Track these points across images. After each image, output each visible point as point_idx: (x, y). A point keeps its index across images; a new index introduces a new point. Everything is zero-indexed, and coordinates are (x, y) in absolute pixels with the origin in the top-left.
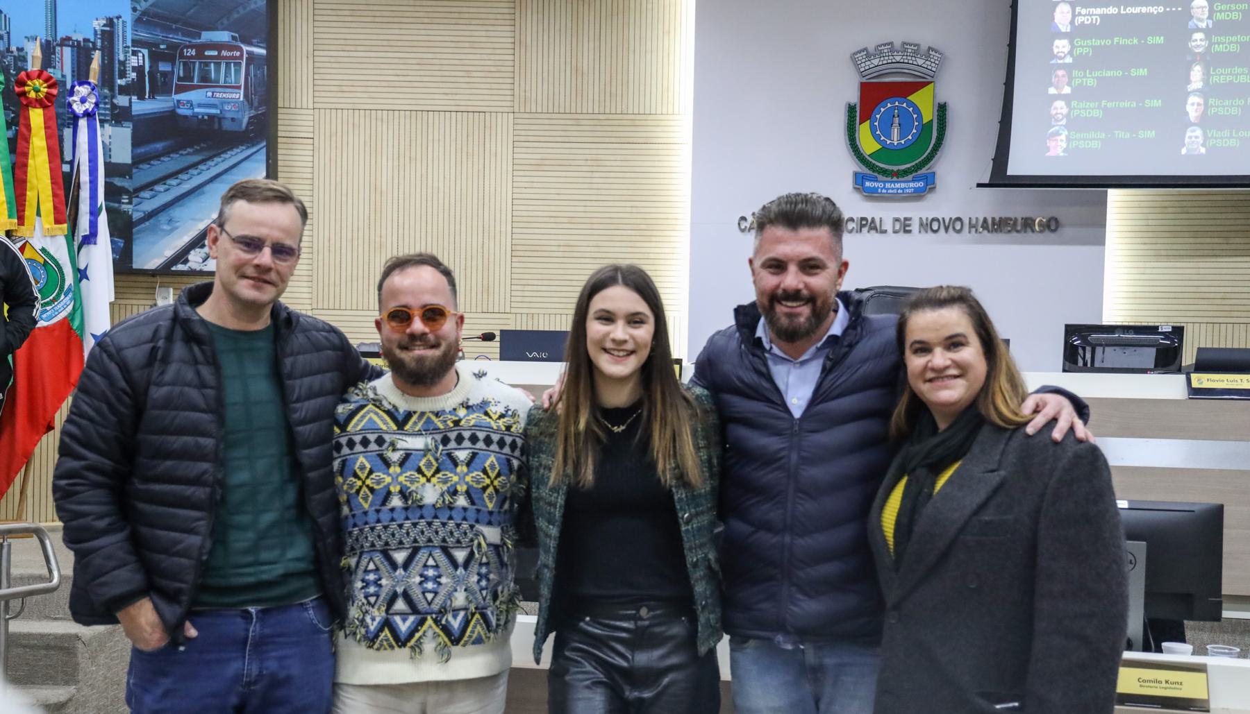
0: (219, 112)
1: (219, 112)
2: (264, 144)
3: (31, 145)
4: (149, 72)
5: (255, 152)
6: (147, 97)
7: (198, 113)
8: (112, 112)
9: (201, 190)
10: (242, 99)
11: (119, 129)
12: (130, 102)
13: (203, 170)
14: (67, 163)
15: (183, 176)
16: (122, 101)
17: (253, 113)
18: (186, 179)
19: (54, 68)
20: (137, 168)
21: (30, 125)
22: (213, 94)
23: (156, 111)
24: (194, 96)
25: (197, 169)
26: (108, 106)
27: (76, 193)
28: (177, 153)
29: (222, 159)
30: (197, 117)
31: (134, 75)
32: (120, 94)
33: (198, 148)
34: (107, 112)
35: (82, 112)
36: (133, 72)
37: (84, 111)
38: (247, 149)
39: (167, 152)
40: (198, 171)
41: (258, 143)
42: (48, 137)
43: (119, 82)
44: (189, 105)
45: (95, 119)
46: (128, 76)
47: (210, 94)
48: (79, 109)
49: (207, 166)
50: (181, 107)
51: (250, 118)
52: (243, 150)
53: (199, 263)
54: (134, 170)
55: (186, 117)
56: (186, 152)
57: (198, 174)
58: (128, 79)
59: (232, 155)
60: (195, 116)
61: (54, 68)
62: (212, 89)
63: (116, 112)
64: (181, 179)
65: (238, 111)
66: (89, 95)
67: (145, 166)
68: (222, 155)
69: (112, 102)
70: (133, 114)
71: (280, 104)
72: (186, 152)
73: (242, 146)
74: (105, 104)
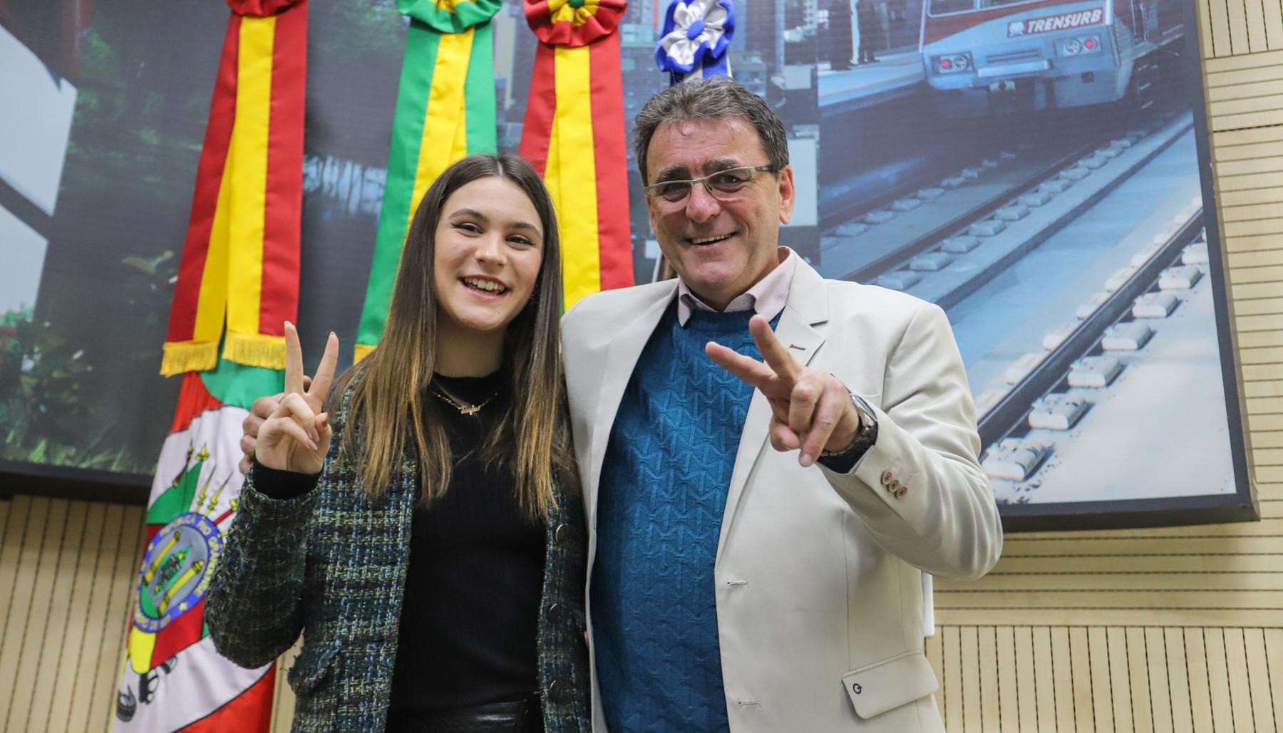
0: (1045, 65)
1: (1045, 65)
2: (1189, 119)
3: (553, 141)
4: (858, 7)
5: (1160, 150)
6: (855, 60)
7: (991, 79)
9: (1009, 271)
10: (1108, 20)
12: (814, 78)
13: (1012, 220)
15: (955, 243)
17: (1145, 48)
18: (964, 248)
19: (638, 21)
20: (832, 235)
22: (1027, 25)
23: (878, 90)
24: (973, 40)
25: (992, 218)
28: (938, 186)
29: (1066, 182)
30: (987, 88)
31: (823, 16)
32: (789, 62)
33: (994, 164)
35: (691, 61)
36: (820, 8)
37: (697, 55)
38: (1132, 145)
39: (907, 188)
40: (997, 223)
41: (1167, 122)
42: (597, 115)
43: (788, 35)
44: (963, 63)
45: (725, 68)
46: (808, 19)
47: (1017, 27)
48: (683, 55)
49: (1020, 209)
50: (942, 71)
51: (1137, 63)
52: (1125, 148)
53: (1015, 481)
54: (825, 242)
55: (955, 93)
56: (960, 180)
57: (998, 232)
58: (808, 27)
59: (1091, 169)
60: (982, 87)
61: (638, 21)
62: (1024, 15)
64: (950, 252)
65: (1101, 54)
66: (709, 13)
67: (853, 229)
68: (1062, 173)
70: (821, 104)
71: (1208, 52)
72: (960, 180)
73: (1120, 138)
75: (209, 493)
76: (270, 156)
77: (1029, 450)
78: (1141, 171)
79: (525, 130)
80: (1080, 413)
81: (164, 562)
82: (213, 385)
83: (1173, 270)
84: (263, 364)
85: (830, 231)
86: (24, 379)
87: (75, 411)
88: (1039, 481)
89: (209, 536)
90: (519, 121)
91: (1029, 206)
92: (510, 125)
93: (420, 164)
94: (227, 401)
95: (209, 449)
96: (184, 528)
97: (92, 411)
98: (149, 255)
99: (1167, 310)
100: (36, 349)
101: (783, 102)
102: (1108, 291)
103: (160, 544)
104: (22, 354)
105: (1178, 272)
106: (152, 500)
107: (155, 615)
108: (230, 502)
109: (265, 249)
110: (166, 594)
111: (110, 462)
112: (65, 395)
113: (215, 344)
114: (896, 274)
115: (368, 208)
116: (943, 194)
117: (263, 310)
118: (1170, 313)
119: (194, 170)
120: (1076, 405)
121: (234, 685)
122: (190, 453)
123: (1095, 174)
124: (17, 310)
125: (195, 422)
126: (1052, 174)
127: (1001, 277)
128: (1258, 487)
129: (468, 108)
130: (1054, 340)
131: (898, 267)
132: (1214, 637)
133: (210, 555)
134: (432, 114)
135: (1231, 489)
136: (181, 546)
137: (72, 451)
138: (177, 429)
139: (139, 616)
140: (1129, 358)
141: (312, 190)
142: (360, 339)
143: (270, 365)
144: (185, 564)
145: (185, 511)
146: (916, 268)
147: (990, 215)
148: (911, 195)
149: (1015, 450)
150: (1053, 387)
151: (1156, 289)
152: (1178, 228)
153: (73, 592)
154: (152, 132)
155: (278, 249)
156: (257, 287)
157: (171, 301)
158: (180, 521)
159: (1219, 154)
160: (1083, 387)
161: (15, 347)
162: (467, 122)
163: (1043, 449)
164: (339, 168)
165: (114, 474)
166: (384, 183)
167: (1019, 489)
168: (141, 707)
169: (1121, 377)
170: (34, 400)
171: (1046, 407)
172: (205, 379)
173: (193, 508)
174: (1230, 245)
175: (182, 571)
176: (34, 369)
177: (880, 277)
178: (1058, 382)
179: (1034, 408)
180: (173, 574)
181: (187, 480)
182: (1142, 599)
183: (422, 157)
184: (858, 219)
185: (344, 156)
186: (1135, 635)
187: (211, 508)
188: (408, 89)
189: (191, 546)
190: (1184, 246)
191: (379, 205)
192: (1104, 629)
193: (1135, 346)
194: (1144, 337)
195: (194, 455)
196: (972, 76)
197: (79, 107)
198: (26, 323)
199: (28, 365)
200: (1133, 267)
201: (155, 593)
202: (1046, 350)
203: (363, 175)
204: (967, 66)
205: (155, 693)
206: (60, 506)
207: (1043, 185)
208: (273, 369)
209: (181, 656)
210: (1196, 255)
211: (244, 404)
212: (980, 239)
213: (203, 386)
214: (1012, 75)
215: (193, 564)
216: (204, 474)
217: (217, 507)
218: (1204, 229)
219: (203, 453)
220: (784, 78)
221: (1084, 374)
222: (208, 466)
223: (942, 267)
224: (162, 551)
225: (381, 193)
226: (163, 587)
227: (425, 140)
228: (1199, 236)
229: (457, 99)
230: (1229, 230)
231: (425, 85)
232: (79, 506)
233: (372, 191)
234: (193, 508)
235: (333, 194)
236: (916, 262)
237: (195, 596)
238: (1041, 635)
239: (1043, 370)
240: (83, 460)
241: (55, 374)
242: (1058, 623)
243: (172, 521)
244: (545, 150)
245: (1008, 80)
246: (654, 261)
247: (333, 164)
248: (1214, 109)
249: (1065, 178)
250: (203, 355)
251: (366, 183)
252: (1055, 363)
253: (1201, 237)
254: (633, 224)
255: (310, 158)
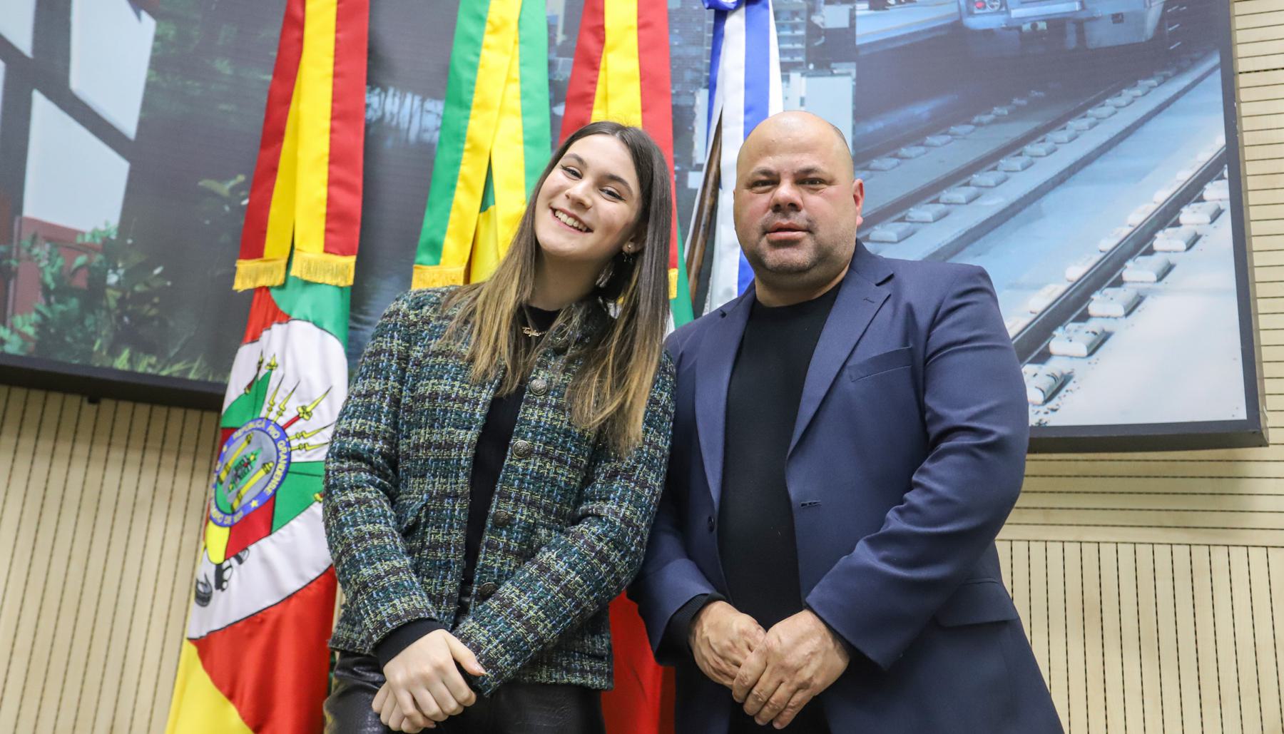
0: (1077, 6)
2: (1216, 60)
3: (602, 74)
8: (807, 45)
9: (1035, 204)
11: (823, 82)
12: (853, 18)
14: (699, 168)
16: (832, 17)
18: (992, 183)
21: (602, 27)
25: (1020, 154)
26: (801, 32)
27: (708, 202)
28: (969, 123)
29: (1093, 120)
30: (1019, 29)
33: (1023, 102)
34: (798, 46)
38: (1159, 85)
39: (939, 124)
41: (1194, 62)
42: (645, 49)
45: (767, 7)
49: (1048, 145)
50: (976, 11)
52: (1152, 87)
55: (988, 33)
56: (992, 117)
57: (1025, 168)
59: (1117, 107)
60: (1014, 28)
63: (817, 44)
67: (887, 163)
68: (1090, 112)
69: (809, 19)
70: (859, 42)
73: (1147, 77)
74: (794, 27)
75: (278, 400)
76: (334, 85)
77: (1048, 375)
78: (1167, 110)
79: (575, 64)
80: (1099, 342)
81: (236, 464)
82: (281, 300)
83: (1195, 206)
84: (328, 281)
85: (863, 165)
86: (110, 292)
87: (156, 323)
88: (1058, 405)
89: (279, 440)
90: (569, 56)
91: (1056, 143)
92: (561, 60)
93: (475, 95)
94: (294, 315)
95: (278, 360)
96: (255, 431)
97: (171, 323)
98: (223, 178)
99: (1187, 244)
100: (120, 265)
101: (823, 39)
102: (1130, 226)
103: (232, 447)
104: (107, 270)
105: (1199, 208)
106: (226, 406)
107: (229, 511)
108: (297, 409)
109: (330, 173)
110: (239, 492)
111: (188, 371)
112: (147, 307)
113: (284, 262)
114: (926, 206)
115: (427, 136)
116: (973, 131)
117: (328, 231)
118: (1189, 248)
119: (264, 99)
120: (1095, 333)
121: (301, 577)
122: (260, 363)
123: (1121, 113)
124: (102, 227)
125: (265, 334)
126: (1078, 112)
127: (1026, 211)
128: (1268, 414)
129: (522, 42)
130: (1076, 271)
131: (928, 200)
132: (1219, 555)
133: (278, 457)
134: (488, 47)
135: (1242, 415)
136: (253, 448)
137: (153, 360)
138: (249, 340)
139: (214, 512)
140: (1149, 289)
141: (374, 119)
142: (418, 259)
143: (334, 282)
144: (256, 465)
145: (256, 416)
146: (945, 201)
147: (1018, 151)
148: (943, 131)
149: (1035, 375)
150: (1074, 316)
151: (1177, 224)
152: (1201, 165)
153: (155, 489)
154: (226, 62)
155: (341, 173)
156: (323, 210)
157: (243, 222)
158: (251, 425)
159: (1243, 95)
160: (1102, 317)
161: (101, 262)
162: (520, 55)
163: (1062, 375)
164: (400, 98)
165: (191, 381)
166: (441, 113)
167: (1038, 412)
168: (216, 593)
169: (1140, 307)
170: (118, 312)
171: (1067, 335)
172: (275, 294)
173: (263, 413)
174: (1251, 183)
175: (253, 471)
176: (119, 282)
177: (911, 209)
178: (1079, 312)
179: (1055, 336)
180: (245, 474)
181: (257, 387)
182: (1152, 518)
183: (478, 88)
184: (892, 153)
185: (406, 87)
186: (1144, 551)
187: (280, 414)
188: (465, 23)
189: (261, 448)
190: (1206, 183)
191: (437, 134)
192: (1115, 545)
193: (1155, 278)
194: (1163, 270)
195: (264, 364)
196: (1005, 16)
197: (157, 38)
198: (111, 240)
199: (112, 279)
200: (1155, 203)
201: (230, 491)
202: (1069, 281)
203: (422, 106)
204: (1001, 7)
205: (230, 582)
206: (143, 409)
207: (1070, 123)
208: (337, 286)
209: (253, 548)
210: (1217, 192)
211: (311, 319)
212: (1008, 174)
213: (273, 301)
214: (1043, 16)
215: (264, 465)
216: (273, 383)
217: (285, 413)
218: (1226, 166)
219: (272, 363)
220: (823, 17)
221: (1104, 304)
222: (277, 375)
223: (971, 200)
224: (235, 452)
225: (439, 123)
226: (236, 486)
227: (481, 71)
228: (1220, 173)
229: (511, 33)
230: (1250, 168)
231: (480, 19)
232: (160, 411)
233: (431, 121)
234: (263, 413)
235: (394, 123)
236: (946, 195)
237: (265, 494)
238: (1055, 549)
239: (1065, 300)
240: (163, 369)
241: (138, 288)
242: (1071, 539)
243: (244, 425)
244: (594, 83)
245: (1044, 20)
246: (696, 190)
247: (394, 95)
248: (1241, 51)
249: (1092, 116)
250: (272, 272)
251: (425, 113)
252: (1077, 294)
253: (1223, 175)
254: (676, 156)
255: (372, 89)
